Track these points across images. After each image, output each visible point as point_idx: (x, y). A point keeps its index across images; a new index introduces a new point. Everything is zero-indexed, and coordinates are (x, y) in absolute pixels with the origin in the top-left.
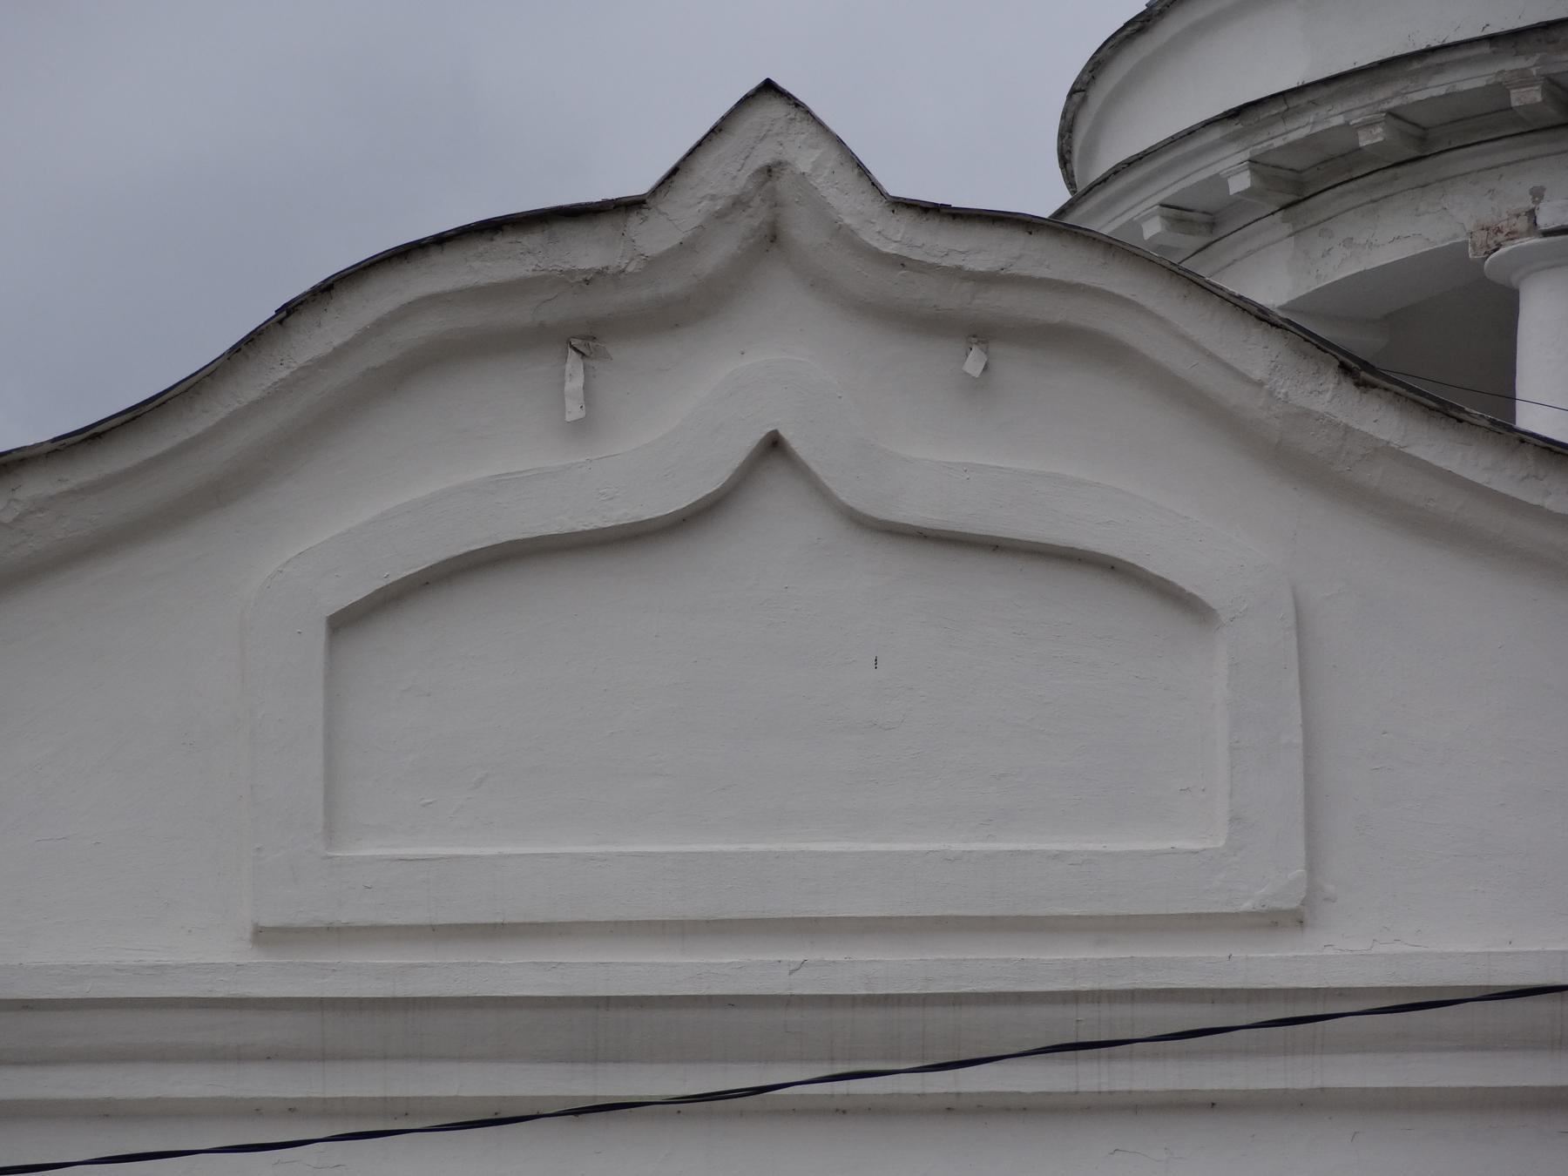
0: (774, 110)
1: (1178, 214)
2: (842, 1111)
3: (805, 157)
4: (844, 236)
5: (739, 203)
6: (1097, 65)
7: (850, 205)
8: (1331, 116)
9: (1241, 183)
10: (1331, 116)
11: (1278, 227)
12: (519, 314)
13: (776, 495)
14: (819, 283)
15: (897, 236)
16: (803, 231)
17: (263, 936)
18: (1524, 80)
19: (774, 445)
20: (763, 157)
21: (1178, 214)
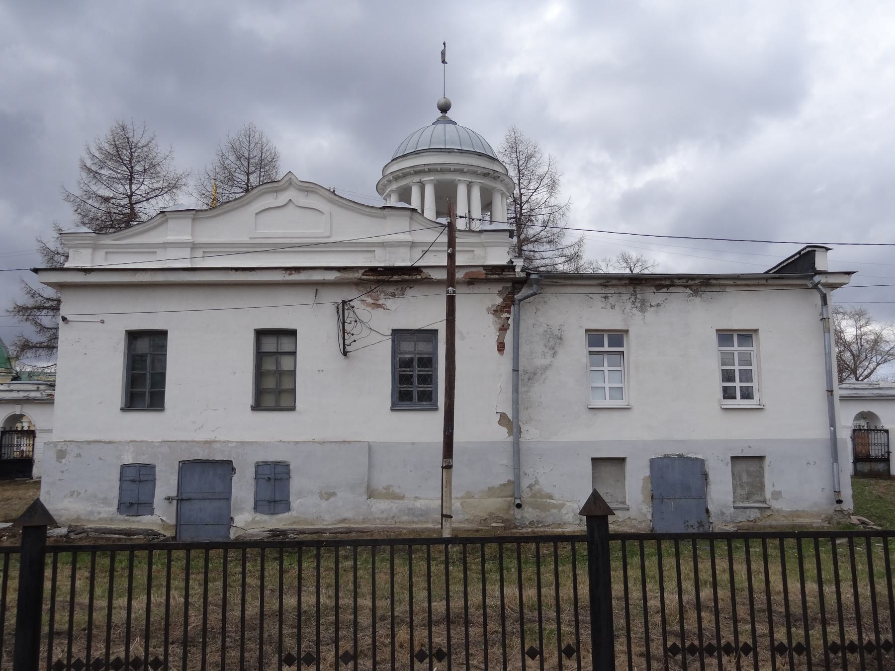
0: (290, 173)
1: (387, 181)
2: (275, 252)
3: (293, 177)
4: (296, 183)
5: (288, 181)
6: (384, 169)
7: (296, 181)
8: (398, 173)
9: (391, 178)
10: (398, 173)
11: (395, 182)
12: (270, 190)
13: (291, 204)
14: (294, 187)
15: (300, 183)
16: (293, 183)
17: (250, 238)
18: (412, 170)
19: (290, 200)
20: (290, 177)
21: (387, 181)
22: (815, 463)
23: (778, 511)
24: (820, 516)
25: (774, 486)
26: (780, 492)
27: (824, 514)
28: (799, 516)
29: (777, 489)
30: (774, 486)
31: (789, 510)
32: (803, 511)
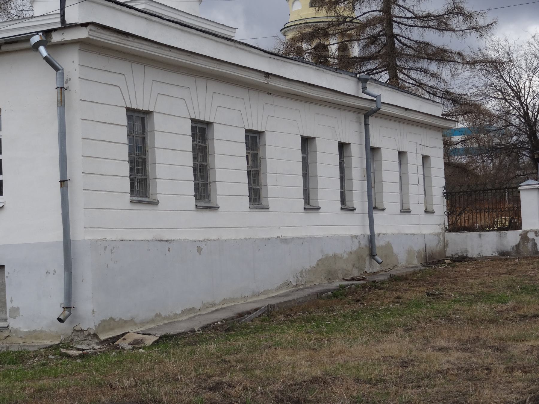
22: (55, 271)
23: (16, 331)
24: (59, 337)
25: (11, 301)
26: (18, 309)
27: (63, 334)
28: (37, 338)
29: (15, 305)
30: (11, 301)
31: (26, 330)
32: (41, 331)
